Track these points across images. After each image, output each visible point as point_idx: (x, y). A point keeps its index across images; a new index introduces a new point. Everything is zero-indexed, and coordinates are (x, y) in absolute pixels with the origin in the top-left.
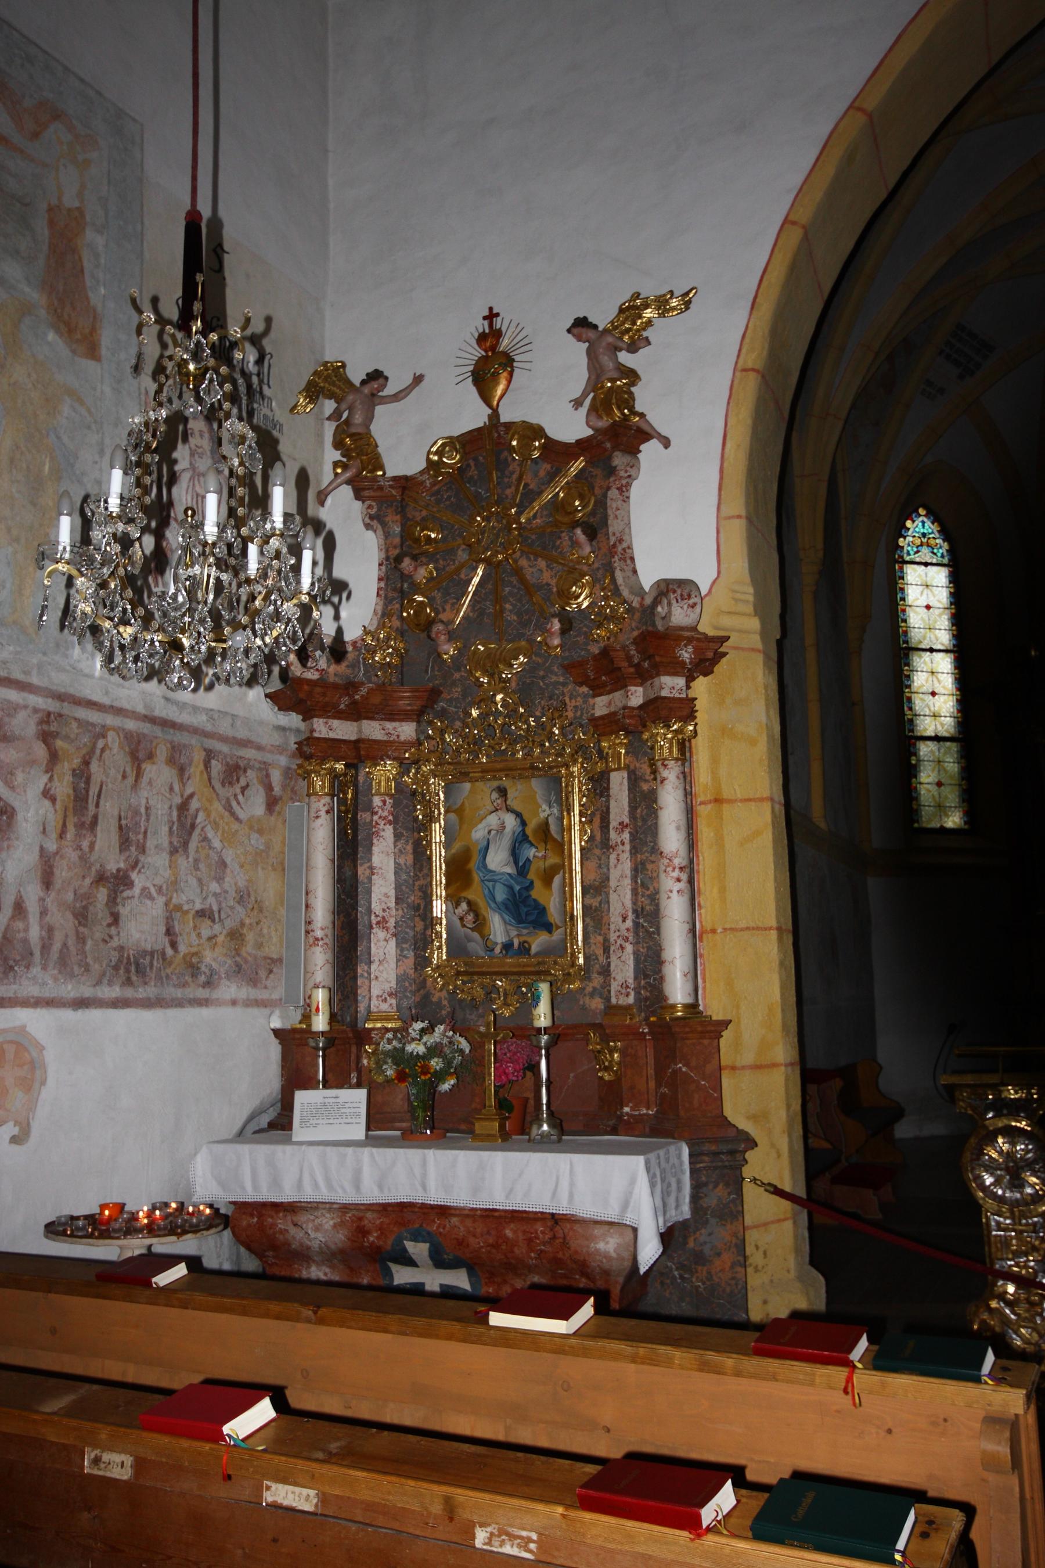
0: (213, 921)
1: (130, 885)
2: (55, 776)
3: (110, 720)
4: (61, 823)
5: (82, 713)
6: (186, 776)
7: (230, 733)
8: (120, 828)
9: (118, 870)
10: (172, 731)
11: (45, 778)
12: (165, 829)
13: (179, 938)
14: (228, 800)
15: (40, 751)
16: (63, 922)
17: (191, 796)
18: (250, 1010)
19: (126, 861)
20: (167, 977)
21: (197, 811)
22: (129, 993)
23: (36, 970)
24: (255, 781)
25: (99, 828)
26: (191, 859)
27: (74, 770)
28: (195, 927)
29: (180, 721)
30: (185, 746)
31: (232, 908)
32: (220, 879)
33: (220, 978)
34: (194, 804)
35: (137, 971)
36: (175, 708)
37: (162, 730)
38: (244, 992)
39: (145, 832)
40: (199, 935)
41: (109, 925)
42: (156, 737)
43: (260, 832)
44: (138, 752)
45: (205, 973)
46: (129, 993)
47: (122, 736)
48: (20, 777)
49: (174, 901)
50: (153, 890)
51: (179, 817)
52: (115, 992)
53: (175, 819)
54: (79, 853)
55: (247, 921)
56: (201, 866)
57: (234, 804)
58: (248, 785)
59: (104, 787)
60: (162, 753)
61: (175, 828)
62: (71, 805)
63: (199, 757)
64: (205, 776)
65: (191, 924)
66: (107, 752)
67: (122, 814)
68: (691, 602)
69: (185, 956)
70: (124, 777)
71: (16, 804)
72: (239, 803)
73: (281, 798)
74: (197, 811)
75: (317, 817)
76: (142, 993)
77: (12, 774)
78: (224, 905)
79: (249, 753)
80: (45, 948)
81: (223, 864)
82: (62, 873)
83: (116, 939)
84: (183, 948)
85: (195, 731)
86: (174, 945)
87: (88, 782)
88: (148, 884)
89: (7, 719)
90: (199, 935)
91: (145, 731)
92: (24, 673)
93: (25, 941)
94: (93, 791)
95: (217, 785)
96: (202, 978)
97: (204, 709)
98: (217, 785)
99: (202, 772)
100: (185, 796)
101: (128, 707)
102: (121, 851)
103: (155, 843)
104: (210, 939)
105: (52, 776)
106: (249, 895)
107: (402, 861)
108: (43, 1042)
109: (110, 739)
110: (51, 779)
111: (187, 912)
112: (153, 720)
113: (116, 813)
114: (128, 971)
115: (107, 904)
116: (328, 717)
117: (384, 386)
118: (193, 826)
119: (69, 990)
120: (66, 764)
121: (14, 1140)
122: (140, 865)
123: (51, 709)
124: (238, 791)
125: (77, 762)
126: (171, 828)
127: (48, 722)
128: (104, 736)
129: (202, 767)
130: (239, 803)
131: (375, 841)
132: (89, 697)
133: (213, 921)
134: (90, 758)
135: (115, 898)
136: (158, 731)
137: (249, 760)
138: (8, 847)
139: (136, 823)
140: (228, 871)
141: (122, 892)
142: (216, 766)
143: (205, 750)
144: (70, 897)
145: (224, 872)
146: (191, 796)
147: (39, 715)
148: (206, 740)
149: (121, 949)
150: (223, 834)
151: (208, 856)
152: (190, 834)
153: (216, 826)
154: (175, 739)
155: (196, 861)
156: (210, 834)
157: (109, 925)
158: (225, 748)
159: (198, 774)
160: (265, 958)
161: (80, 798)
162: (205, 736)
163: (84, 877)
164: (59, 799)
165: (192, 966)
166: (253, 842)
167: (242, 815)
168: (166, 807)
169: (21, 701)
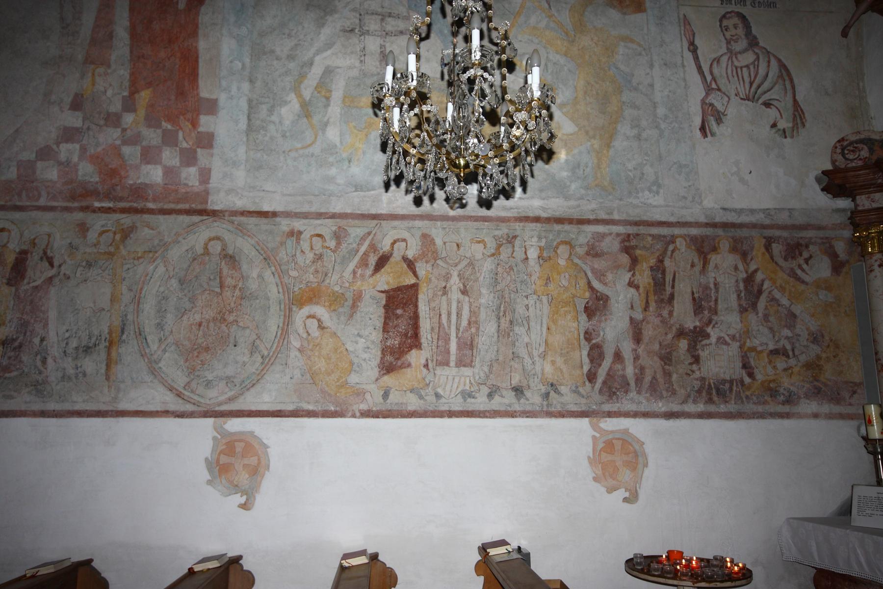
0: (788, 357)
1: (708, 336)
3: (677, 231)
4: (645, 301)
5: (655, 231)
6: (749, 258)
7: (789, 222)
8: (694, 299)
9: (695, 327)
10: (733, 230)
11: (629, 275)
12: (734, 297)
13: (756, 371)
14: (792, 269)
15: (625, 259)
16: (653, 364)
17: (756, 271)
18: (834, 422)
19: (700, 321)
20: (747, 397)
21: (763, 281)
22: (712, 408)
23: (633, 394)
24: (818, 252)
25: (675, 301)
26: (760, 315)
27: (651, 267)
28: (770, 362)
30: (746, 238)
31: (806, 347)
32: (791, 327)
33: (799, 398)
34: (759, 276)
35: (718, 394)
36: (733, 214)
38: (826, 408)
39: (716, 300)
40: (775, 367)
41: (691, 364)
43: (829, 289)
44: (704, 248)
45: (783, 394)
46: (712, 408)
47: (688, 240)
48: (610, 276)
49: (748, 344)
50: (727, 339)
51: (746, 287)
52: (701, 407)
54: (660, 318)
55: (824, 355)
56: (771, 319)
57: (799, 272)
58: (811, 257)
60: (725, 245)
61: (743, 295)
62: (652, 289)
64: (767, 256)
65: (766, 360)
66: (677, 252)
67: (695, 291)
69: (763, 383)
70: (693, 266)
71: (609, 293)
72: (803, 270)
73: (848, 261)
74: (763, 281)
75: (871, 271)
76: (723, 408)
77: (604, 276)
78: (797, 345)
79: (810, 234)
80: (639, 380)
81: (794, 316)
82: (648, 332)
83: (698, 373)
84: (759, 377)
85: (754, 226)
86: (751, 375)
87: (664, 272)
88: (722, 335)
89: (597, 244)
90: (775, 367)
91: (708, 233)
92: (608, 214)
93: (624, 376)
94: (669, 278)
95: (781, 262)
96: (782, 398)
97: (760, 210)
98: (781, 262)
99: (763, 254)
101: (692, 220)
102: (695, 314)
103: (726, 306)
104: (785, 370)
106: (823, 336)
108: (642, 440)
109: (678, 243)
110: (633, 275)
111: (761, 352)
112: (714, 225)
113: (689, 291)
114: (709, 393)
115: (688, 350)
118: (760, 292)
119: (661, 406)
120: (644, 264)
121: (625, 500)
122: (713, 322)
123: (630, 232)
124: (802, 262)
125: (653, 262)
126: (739, 296)
127: (629, 241)
129: (763, 250)
130: (803, 270)
133: (788, 357)
135: (696, 345)
136: (720, 232)
137: (811, 238)
138: (606, 320)
141: (700, 341)
142: (777, 248)
143: (765, 238)
144: (656, 347)
146: (756, 271)
147: (622, 237)
148: (765, 231)
149: (703, 379)
153: (782, 289)
155: (766, 317)
156: (777, 294)
157: (691, 364)
158: (785, 234)
160: (846, 382)
161: (659, 285)
163: (666, 334)
164: (641, 286)
165: (770, 389)
167: (807, 278)
168: (733, 281)
169: (607, 231)
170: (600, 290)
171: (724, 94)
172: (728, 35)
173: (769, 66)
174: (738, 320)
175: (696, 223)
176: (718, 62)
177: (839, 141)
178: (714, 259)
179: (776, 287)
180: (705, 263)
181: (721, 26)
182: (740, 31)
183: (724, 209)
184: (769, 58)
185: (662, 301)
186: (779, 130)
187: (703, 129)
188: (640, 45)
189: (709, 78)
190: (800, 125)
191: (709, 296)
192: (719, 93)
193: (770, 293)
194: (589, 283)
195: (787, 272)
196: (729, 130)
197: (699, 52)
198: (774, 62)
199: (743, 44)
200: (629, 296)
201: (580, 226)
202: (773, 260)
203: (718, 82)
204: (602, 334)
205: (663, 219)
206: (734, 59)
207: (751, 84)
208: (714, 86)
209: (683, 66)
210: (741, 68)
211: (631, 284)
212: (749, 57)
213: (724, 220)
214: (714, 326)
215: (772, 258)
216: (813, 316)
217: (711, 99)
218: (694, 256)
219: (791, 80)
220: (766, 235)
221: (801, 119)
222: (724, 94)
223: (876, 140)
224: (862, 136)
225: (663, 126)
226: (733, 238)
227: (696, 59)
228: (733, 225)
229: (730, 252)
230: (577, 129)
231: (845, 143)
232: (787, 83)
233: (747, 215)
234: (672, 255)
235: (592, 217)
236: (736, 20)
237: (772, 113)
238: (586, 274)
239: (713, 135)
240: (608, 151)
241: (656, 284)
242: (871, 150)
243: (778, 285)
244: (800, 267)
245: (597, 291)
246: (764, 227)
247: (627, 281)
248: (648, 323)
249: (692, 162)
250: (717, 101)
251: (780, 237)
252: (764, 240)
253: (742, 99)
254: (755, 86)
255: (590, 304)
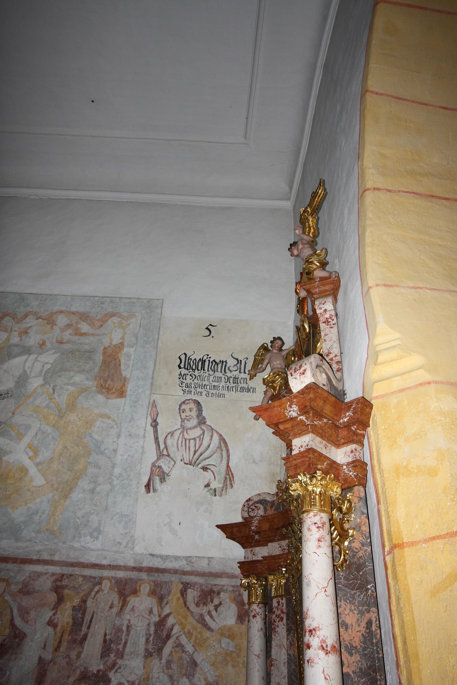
2: (59, 611)
5: (87, 572)
6: (165, 603)
8: (105, 641)
9: (99, 671)
10: (156, 574)
11: (51, 613)
12: (143, 640)
14: (202, 615)
17: (168, 615)
19: (105, 664)
21: (173, 626)
24: (228, 600)
25: (87, 642)
26: (164, 661)
27: (74, 607)
29: (163, 567)
30: (166, 583)
34: (171, 621)
36: (159, 559)
37: (148, 575)
39: (126, 643)
42: (141, 580)
43: (231, 637)
47: (113, 582)
53: (152, 632)
56: (174, 666)
57: (207, 618)
58: (220, 604)
59: (95, 615)
60: (145, 589)
61: (151, 639)
62: (69, 629)
63: (176, 589)
64: (181, 600)
66: (101, 593)
67: (108, 632)
68: (301, 371)
70: (111, 607)
72: (212, 617)
74: (173, 626)
77: (28, 613)
79: (224, 581)
81: (194, 664)
85: (176, 572)
89: (32, 582)
91: (133, 577)
92: (50, 555)
94: (87, 618)
95: (193, 607)
97: (184, 557)
99: (178, 598)
100: (162, 616)
101: (122, 564)
102: (101, 657)
105: (56, 611)
107: (291, 652)
109: (103, 585)
110: (54, 614)
112: (140, 569)
113: (102, 632)
116: (251, 547)
117: (283, 344)
118: (168, 637)
122: (117, 667)
123: (65, 572)
124: (212, 608)
125: (76, 601)
126: (147, 641)
127: (61, 581)
128: (100, 583)
129: (179, 595)
130: (212, 617)
131: (273, 636)
132: (94, 562)
134: (87, 598)
136: (144, 576)
137: (223, 586)
138: (15, 659)
139: (118, 637)
140: (198, 669)
142: (192, 594)
143: (182, 583)
145: (194, 670)
146: (168, 615)
147: (55, 577)
150: (195, 641)
151: (181, 658)
152: (165, 642)
153: (189, 635)
154: (159, 579)
155: (169, 662)
156: (184, 640)
158: (201, 580)
159: (175, 600)
162: (184, 574)
163: (69, 677)
164: (60, 625)
166: (223, 645)
169: (44, 571)
170: (20, 628)
171: (172, 459)
172: (183, 415)
173: (211, 439)
174: (141, 665)
175: (125, 566)
176: (172, 435)
177: (247, 501)
178: (133, 601)
179: (184, 633)
180: (124, 604)
181: (179, 409)
182: (194, 413)
183: (152, 555)
184: (212, 433)
185: (74, 641)
186: (211, 489)
187: (148, 486)
188: (114, 420)
189: (162, 446)
190: (229, 485)
191: (119, 638)
192: (168, 458)
193: (177, 638)
194: (12, 620)
195: (197, 617)
196: (169, 488)
197: (159, 427)
198: (216, 437)
199: (195, 422)
200: (45, 635)
201: (21, 565)
202: (185, 605)
203: (169, 450)
204: (8, 673)
205: (97, 562)
206: (185, 433)
207: (195, 452)
208: (165, 452)
209: (144, 437)
210: (190, 440)
211: (51, 623)
212: (197, 432)
213: (151, 565)
214: (116, 671)
215: (185, 603)
216: (213, 665)
217: (161, 463)
218: (115, 598)
219: (228, 451)
220: (184, 581)
221: (230, 480)
222: (172, 459)
223: (269, 502)
224: (261, 498)
225: (115, 483)
226: (154, 582)
227: (156, 431)
228: (158, 570)
229: (148, 595)
230: (45, 482)
231: (251, 503)
232: (224, 452)
233: (171, 562)
234: (95, 596)
235: (35, 558)
236: (192, 405)
237: (208, 475)
238: (12, 611)
239: (154, 491)
240: (65, 501)
241: (74, 624)
242: (265, 510)
243: (186, 630)
244: (209, 613)
245: (17, 629)
246: (184, 573)
247: (47, 619)
248: (55, 664)
249: (132, 513)
250: (165, 464)
251: (196, 583)
252: (181, 586)
253: (185, 463)
254: (198, 454)
255: (6, 641)
